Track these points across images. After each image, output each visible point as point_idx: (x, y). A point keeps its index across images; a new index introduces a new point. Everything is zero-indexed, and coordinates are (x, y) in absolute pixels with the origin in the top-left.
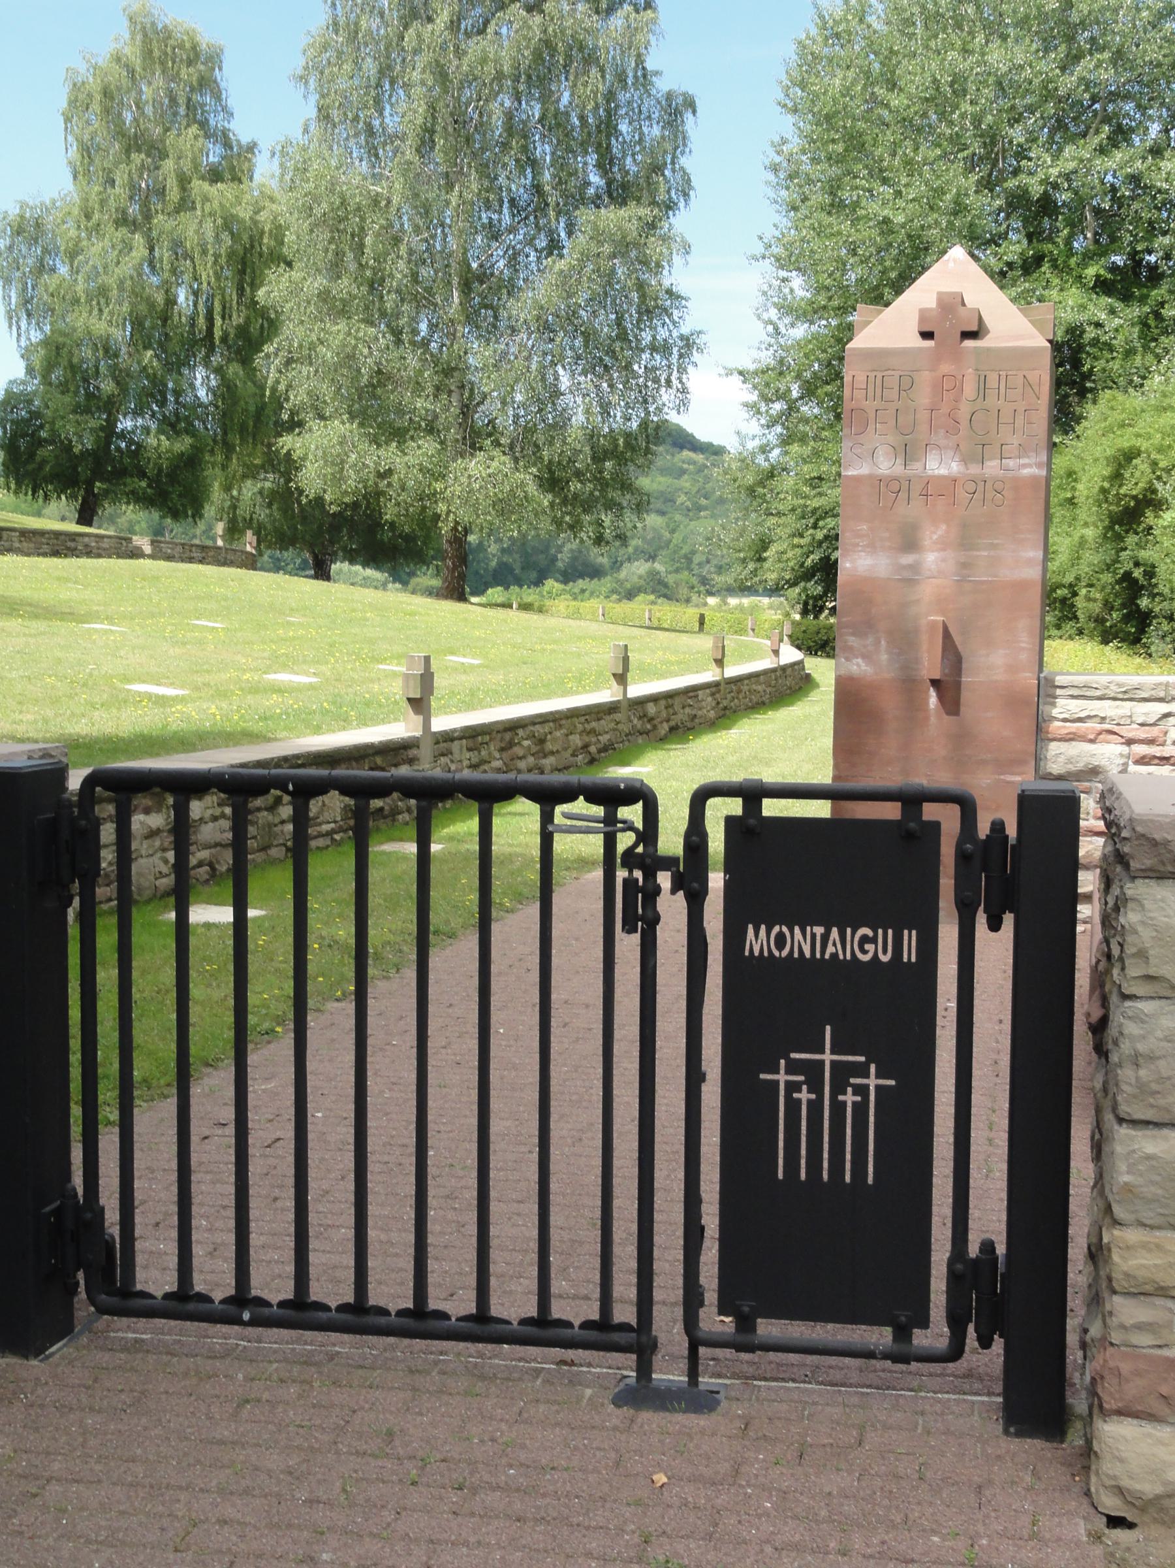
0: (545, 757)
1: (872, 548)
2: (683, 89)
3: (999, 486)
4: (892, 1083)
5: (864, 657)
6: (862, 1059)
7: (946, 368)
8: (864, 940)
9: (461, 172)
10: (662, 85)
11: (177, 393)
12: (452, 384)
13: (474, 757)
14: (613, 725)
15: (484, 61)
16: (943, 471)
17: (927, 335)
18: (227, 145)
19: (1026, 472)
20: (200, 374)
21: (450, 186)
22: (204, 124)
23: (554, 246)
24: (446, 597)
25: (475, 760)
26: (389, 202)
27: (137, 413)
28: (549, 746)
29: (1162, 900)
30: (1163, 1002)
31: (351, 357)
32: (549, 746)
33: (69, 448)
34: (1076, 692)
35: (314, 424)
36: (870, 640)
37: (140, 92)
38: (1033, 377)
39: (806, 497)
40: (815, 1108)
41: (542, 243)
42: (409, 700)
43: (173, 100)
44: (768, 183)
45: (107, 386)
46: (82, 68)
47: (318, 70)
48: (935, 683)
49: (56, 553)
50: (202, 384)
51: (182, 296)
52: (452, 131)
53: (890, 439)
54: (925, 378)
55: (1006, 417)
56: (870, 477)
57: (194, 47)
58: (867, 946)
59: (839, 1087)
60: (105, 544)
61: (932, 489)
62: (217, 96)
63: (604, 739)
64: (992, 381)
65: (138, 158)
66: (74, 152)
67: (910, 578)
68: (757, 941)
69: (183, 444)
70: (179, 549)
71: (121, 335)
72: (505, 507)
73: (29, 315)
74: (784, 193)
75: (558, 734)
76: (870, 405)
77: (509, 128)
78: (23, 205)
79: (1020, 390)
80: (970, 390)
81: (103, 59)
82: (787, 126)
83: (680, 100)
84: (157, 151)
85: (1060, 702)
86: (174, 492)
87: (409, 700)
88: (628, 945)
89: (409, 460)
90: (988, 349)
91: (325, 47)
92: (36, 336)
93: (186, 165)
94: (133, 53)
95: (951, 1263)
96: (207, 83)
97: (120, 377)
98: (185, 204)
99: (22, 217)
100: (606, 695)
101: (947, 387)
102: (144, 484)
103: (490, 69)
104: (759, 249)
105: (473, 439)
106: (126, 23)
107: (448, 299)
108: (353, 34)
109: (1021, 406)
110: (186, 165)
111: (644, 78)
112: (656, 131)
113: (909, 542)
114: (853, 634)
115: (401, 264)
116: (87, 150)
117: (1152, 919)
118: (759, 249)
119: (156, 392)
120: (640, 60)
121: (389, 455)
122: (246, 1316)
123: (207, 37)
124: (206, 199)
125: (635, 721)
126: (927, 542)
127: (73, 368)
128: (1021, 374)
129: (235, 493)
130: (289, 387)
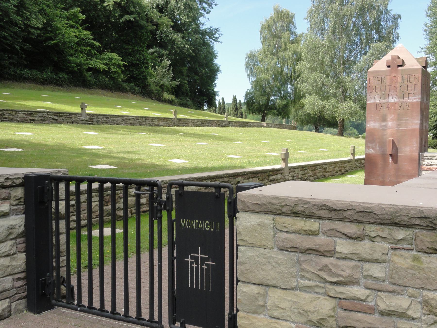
0: (326, 173)
1: (375, 121)
2: (398, 13)
3: (408, 104)
4: (214, 263)
5: (373, 149)
6: (207, 257)
7: (394, 75)
8: (207, 224)
9: (342, 37)
10: (392, 13)
11: (284, 91)
12: (340, 86)
13: (303, 173)
14: (350, 165)
15: (347, 11)
16: (393, 101)
17: (389, 67)
18: (295, 35)
19: (415, 100)
20: (289, 86)
21: (339, 40)
22: (290, 31)
23: (365, 54)
24: (339, 135)
25: (302, 173)
26: (326, 45)
27: (275, 95)
28: (328, 170)
29: (245, 218)
30: (248, 247)
31: (316, 81)
32: (328, 170)
33: (259, 104)
34: (430, 158)
35: (308, 96)
36: (374, 144)
37: (276, 25)
38: (417, 76)
39: (432, 110)
40: (197, 268)
41: (363, 52)
42: (282, 159)
43: (284, 26)
44: (423, 34)
45: (268, 90)
46: (264, 21)
47: (310, 16)
48: (391, 155)
49: (243, 126)
50: (289, 88)
51: (285, 69)
52: (342, 28)
53: (379, 93)
54: (388, 78)
55: (410, 87)
56: (374, 103)
57: (288, 14)
58: (208, 226)
59: (202, 264)
60: (255, 124)
61: (390, 106)
62: (293, 24)
63: (347, 169)
64: (406, 78)
65: (275, 39)
66: (262, 39)
67: (384, 128)
68: (183, 223)
69: (285, 102)
70: (273, 125)
71: (271, 79)
72: (352, 114)
73: (252, 75)
74: (428, 36)
75: (331, 167)
76: (374, 85)
77: (354, 26)
78: (251, 51)
79: (413, 79)
80: (400, 80)
81: (268, 19)
82: (428, 21)
83: (397, 16)
84: (279, 37)
85: (425, 160)
86: (283, 112)
87: (282, 159)
88: (156, 222)
89: (329, 104)
90: (407, 69)
91: (311, 11)
92: (253, 79)
93: (286, 40)
94: (275, 17)
95: (229, 314)
96: (291, 22)
97: (271, 88)
98: (286, 49)
99: (251, 54)
100: (350, 158)
101: (394, 80)
102: (276, 111)
103: (349, 12)
104: (420, 50)
105: (345, 97)
106: (273, 10)
107: (339, 66)
108: (317, 7)
109: (414, 84)
110: (286, 40)
111: (387, 12)
112: (391, 24)
113: (384, 119)
114: (370, 143)
115: (328, 59)
116: (265, 39)
117: (242, 223)
118: (420, 50)
119: (279, 91)
120: (386, 7)
121: (325, 103)
122: (79, 309)
123: (291, 11)
124: (290, 48)
125: (357, 164)
126: (389, 119)
127: (261, 86)
128: (413, 75)
129: (297, 112)
130: (302, 88)
